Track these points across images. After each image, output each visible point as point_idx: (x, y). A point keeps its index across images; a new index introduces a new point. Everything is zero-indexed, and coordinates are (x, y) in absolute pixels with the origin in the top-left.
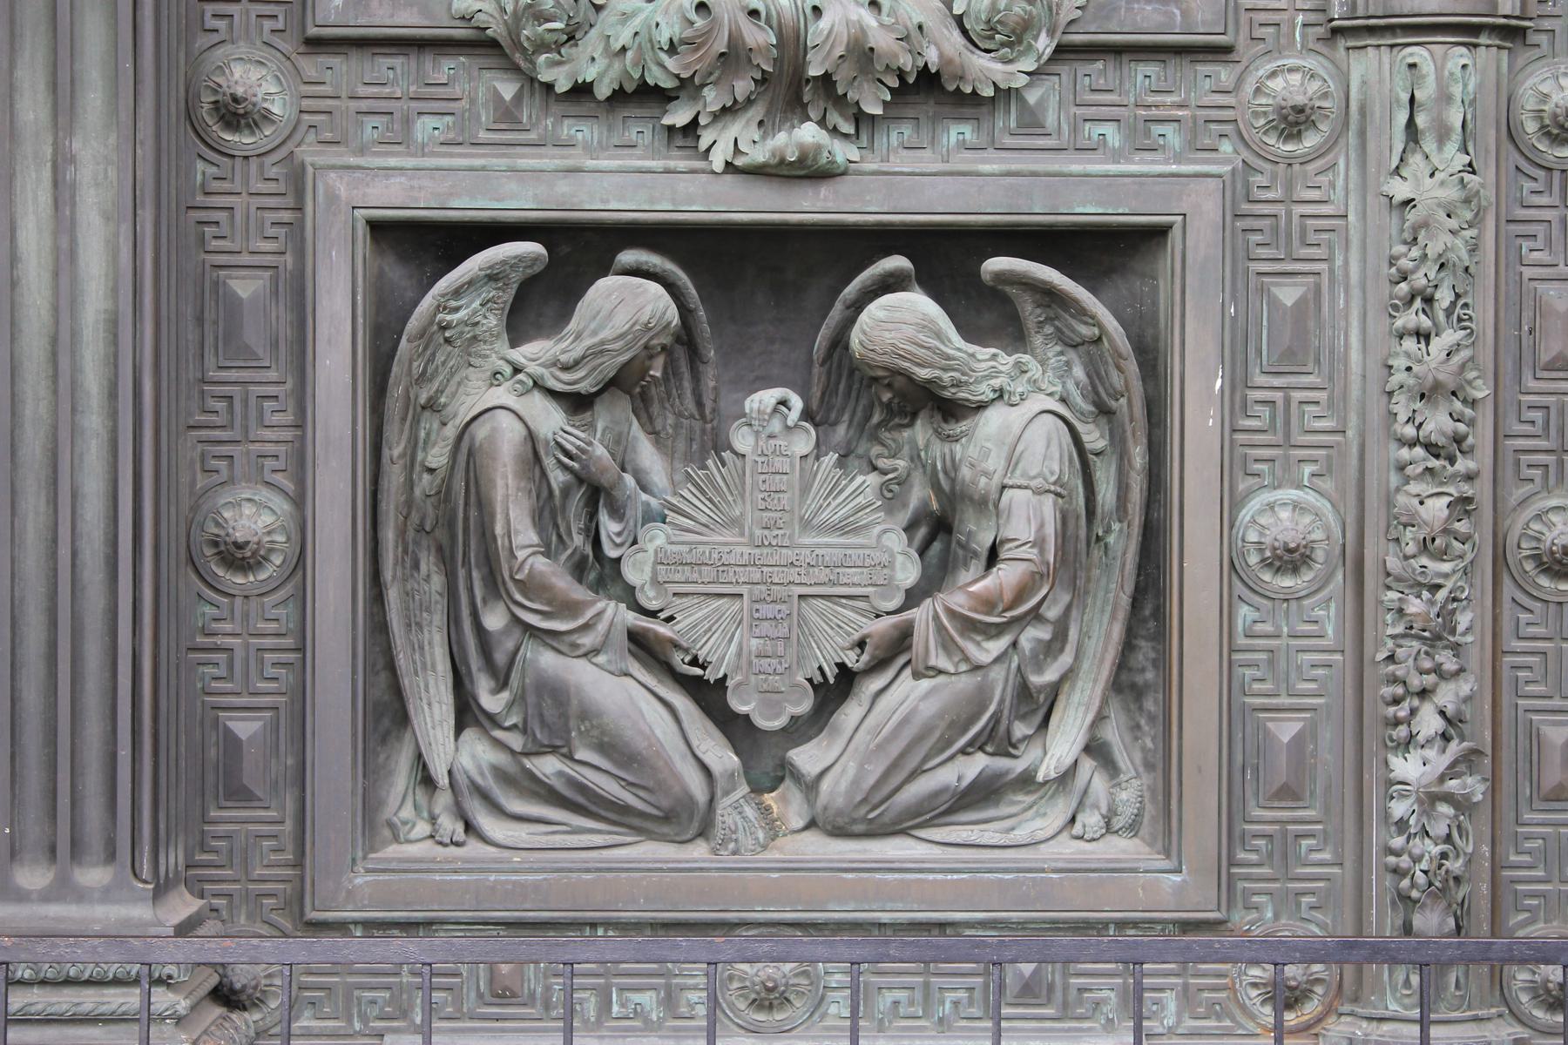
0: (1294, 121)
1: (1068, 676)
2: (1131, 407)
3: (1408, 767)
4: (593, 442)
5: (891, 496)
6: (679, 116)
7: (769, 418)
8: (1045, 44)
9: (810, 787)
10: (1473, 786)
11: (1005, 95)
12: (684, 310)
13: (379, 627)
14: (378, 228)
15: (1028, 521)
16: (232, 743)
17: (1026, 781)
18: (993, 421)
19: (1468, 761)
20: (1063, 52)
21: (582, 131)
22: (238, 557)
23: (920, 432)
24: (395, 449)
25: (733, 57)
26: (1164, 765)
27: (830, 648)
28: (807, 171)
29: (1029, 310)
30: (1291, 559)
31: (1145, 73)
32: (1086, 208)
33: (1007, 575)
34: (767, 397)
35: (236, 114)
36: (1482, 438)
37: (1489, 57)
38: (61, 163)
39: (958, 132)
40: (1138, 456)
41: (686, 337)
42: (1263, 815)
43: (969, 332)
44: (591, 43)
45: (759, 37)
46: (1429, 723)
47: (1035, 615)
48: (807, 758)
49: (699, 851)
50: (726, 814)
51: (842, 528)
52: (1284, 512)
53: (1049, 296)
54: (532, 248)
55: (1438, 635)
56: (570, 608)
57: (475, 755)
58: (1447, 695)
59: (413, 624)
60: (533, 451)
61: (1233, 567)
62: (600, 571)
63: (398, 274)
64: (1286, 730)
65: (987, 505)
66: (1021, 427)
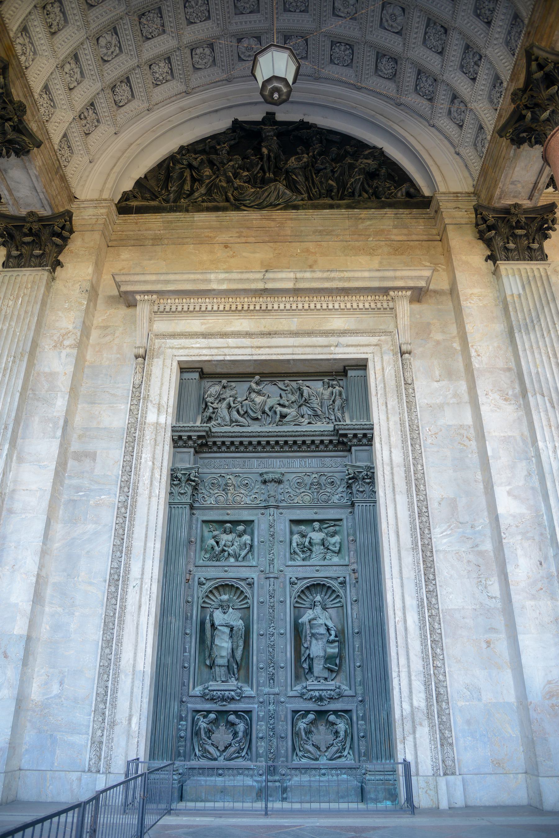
4: (209, 726)
15: (241, 734)
25: (219, 697)
27: (226, 745)
28: (224, 705)
33: (238, 739)
62: (209, 738)
64: (261, 752)
66: (241, 727)
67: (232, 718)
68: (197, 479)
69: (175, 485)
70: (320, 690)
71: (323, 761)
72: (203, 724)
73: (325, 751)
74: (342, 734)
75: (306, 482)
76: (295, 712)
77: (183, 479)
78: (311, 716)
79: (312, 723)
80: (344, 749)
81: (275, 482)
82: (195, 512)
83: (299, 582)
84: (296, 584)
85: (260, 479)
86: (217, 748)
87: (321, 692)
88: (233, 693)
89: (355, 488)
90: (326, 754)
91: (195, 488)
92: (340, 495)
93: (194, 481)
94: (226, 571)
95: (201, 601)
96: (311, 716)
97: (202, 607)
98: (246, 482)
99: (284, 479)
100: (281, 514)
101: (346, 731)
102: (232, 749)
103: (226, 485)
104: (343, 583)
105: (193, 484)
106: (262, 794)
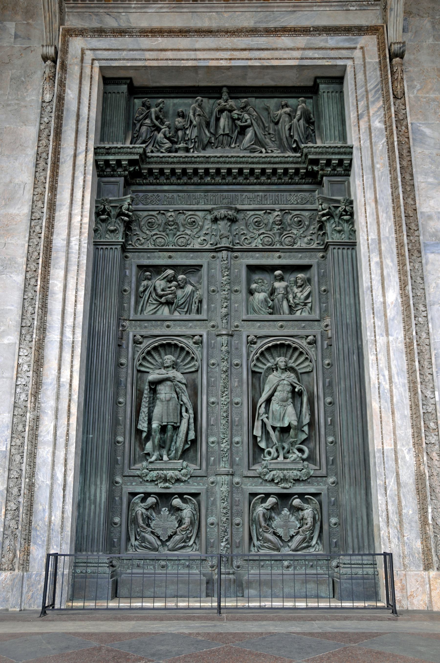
0: (212, 483)
1: (192, 536)
2: (197, 510)
3: (223, 544)
5: (176, 518)
6: (156, 483)
7: (165, 511)
8: (189, 476)
9: (168, 546)
10: (229, 546)
11: (185, 481)
12: (157, 500)
13: (128, 531)
14: (129, 493)
15: (187, 521)
16: (114, 541)
17: (188, 546)
18: (185, 511)
19: (228, 544)
20: (191, 477)
21: (148, 484)
22: (116, 524)
23: (179, 512)
24: (130, 514)
25: (161, 478)
26: (200, 544)
27: (170, 533)
29: (188, 500)
30: (212, 524)
31: (199, 478)
32: (193, 491)
34: (164, 509)
35: (117, 483)
36: (229, 512)
37: (230, 477)
38: (101, 487)
39: (182, 484)
40: (198, 514)
41: (157, 503)
42: (209, 549)
43: (184, 502)
44: (148, 476)
45: (163, 476)
46: (224, 540)
47: (188, 529)
48: (168, 544)
49: (157, 553)
50: (160, 549)
51: (171, 521)
52: (212, 519)
53: (190, 499)
54: (143, 495)
55: (226, 531)
56: (145, 529)
57: (137, 543)
58: (226, 537)
59: (131, 530)
60: (142, 514)
61: (206, 524)
63: (131, 497)
64: (212, 541)
65: (184, 519)
66: (187, 512)
67: (176, 502)
68: (131, 214)
69: (103, 221)
70: (284, 469)
71: (286, 551)
72: (140, 509)
73: (289, 541)
74: (310, 521)
75: (266, 221)
76: (253, 495)
77: (114, 213)
78: (272, 500)
79: (273, 509)
80: (312, 538)
81: (229, 220)
82: (128, 255)
83: (259, 341)
84: (255, 343)
85: (209, 217)
86: (158, 537)
87: (285, 472)
88: (177, 473)
89: (329, 227)
90: (290, 544)
91: (128, 226)
92: (309, 238)
93: (127, 216)
94: (168, 327)
95: (137, 363)
96: (272, 500)
97: (139, 371)
98: (192, 220)
99: (240, 216)
100: (236, 257)
101: (314, 518)
102: (177, 538)
103: (167, 223)
104: (313, 343)
105: (126, 218)
106: (211, 587)
